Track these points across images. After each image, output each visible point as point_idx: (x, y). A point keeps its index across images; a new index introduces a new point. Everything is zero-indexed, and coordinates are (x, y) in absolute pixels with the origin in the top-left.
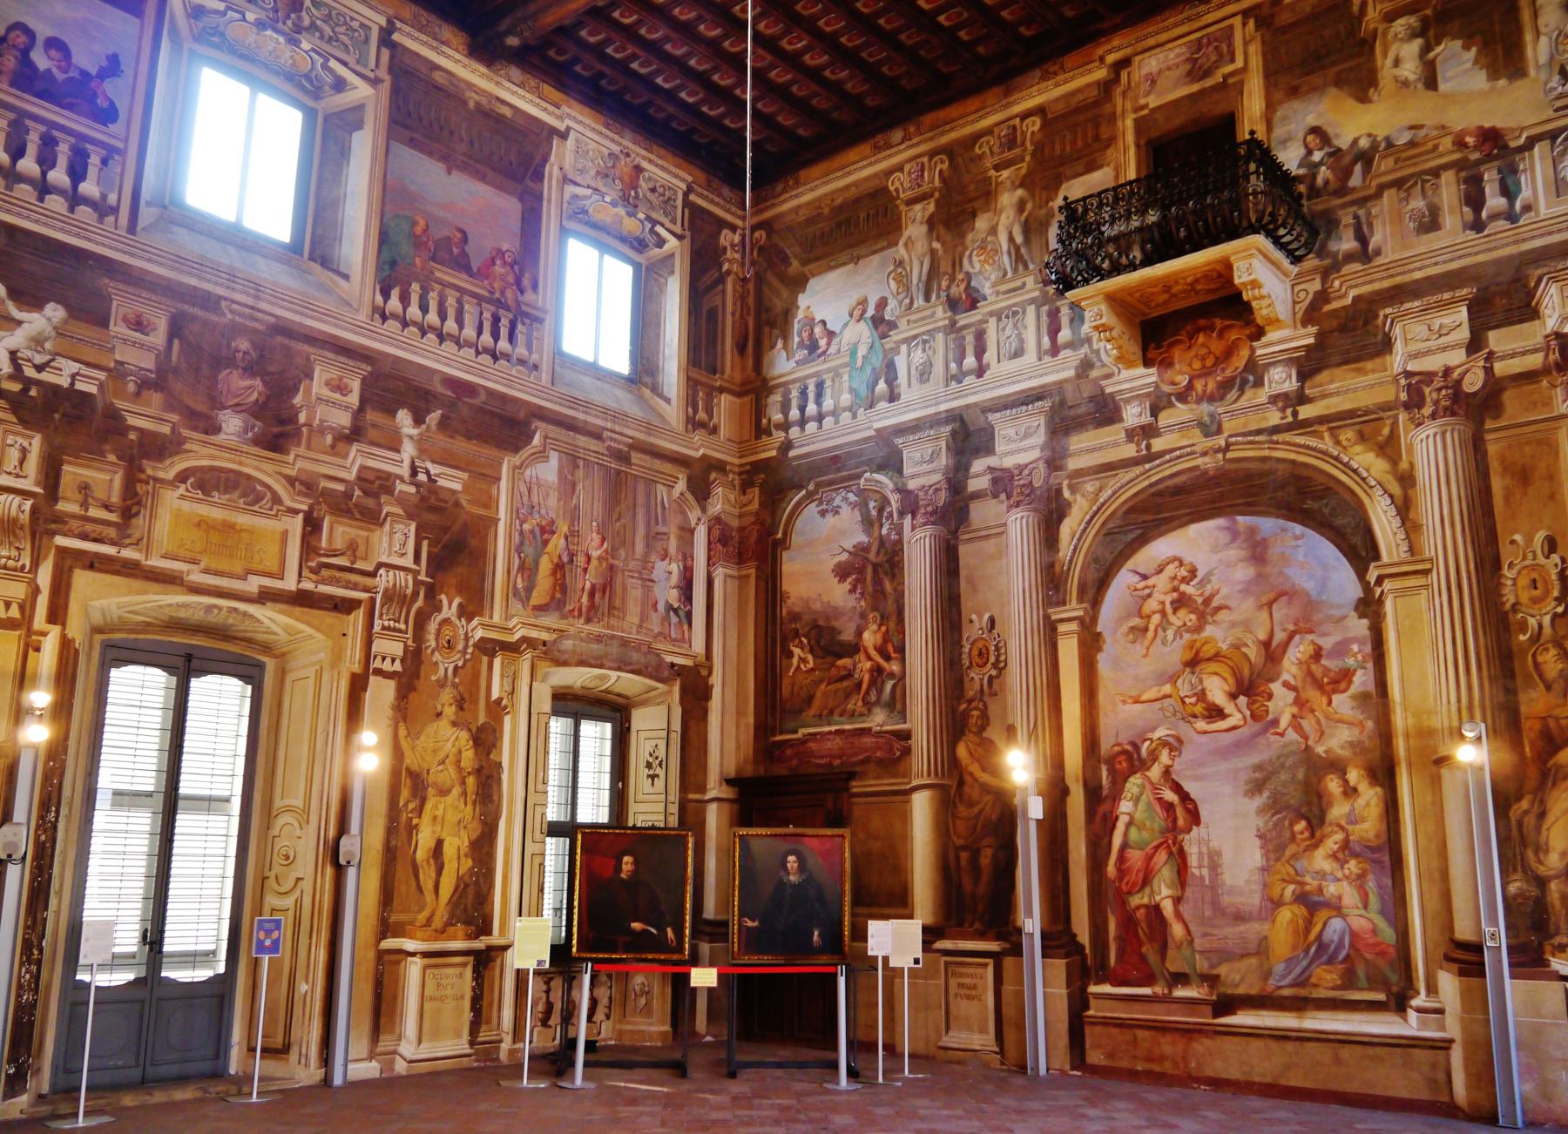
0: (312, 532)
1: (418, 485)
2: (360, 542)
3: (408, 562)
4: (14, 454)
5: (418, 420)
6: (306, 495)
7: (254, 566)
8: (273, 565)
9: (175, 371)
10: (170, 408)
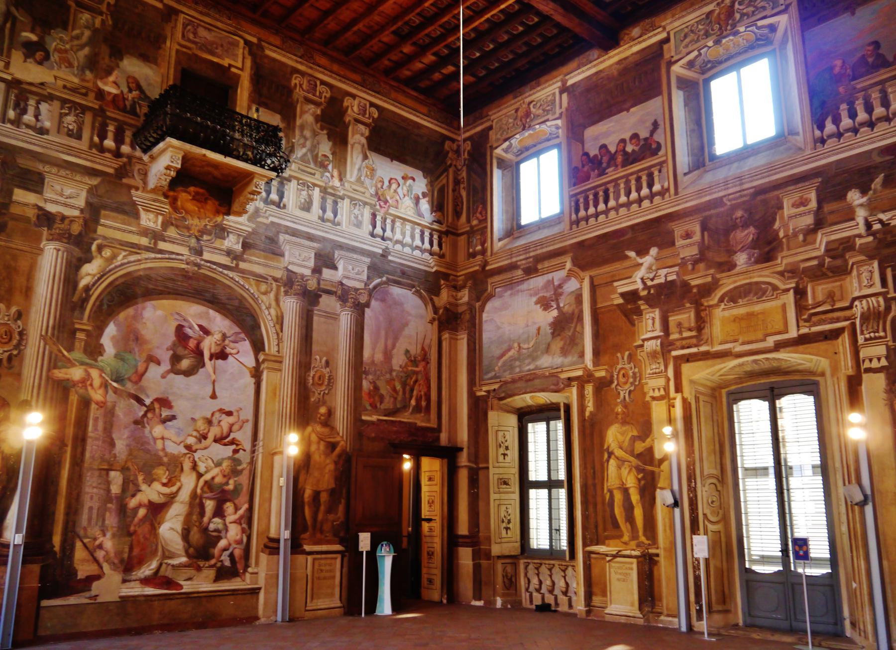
0: (801, 298)
1: (874, 234)
2: (836, 290)
3: (878, 288)
4: (650, 322)
5: (864, 191)
6: (793, 278)
7: (769, 331)
8: (779, 326)
9: (708, 248)
10: (708, 267)
